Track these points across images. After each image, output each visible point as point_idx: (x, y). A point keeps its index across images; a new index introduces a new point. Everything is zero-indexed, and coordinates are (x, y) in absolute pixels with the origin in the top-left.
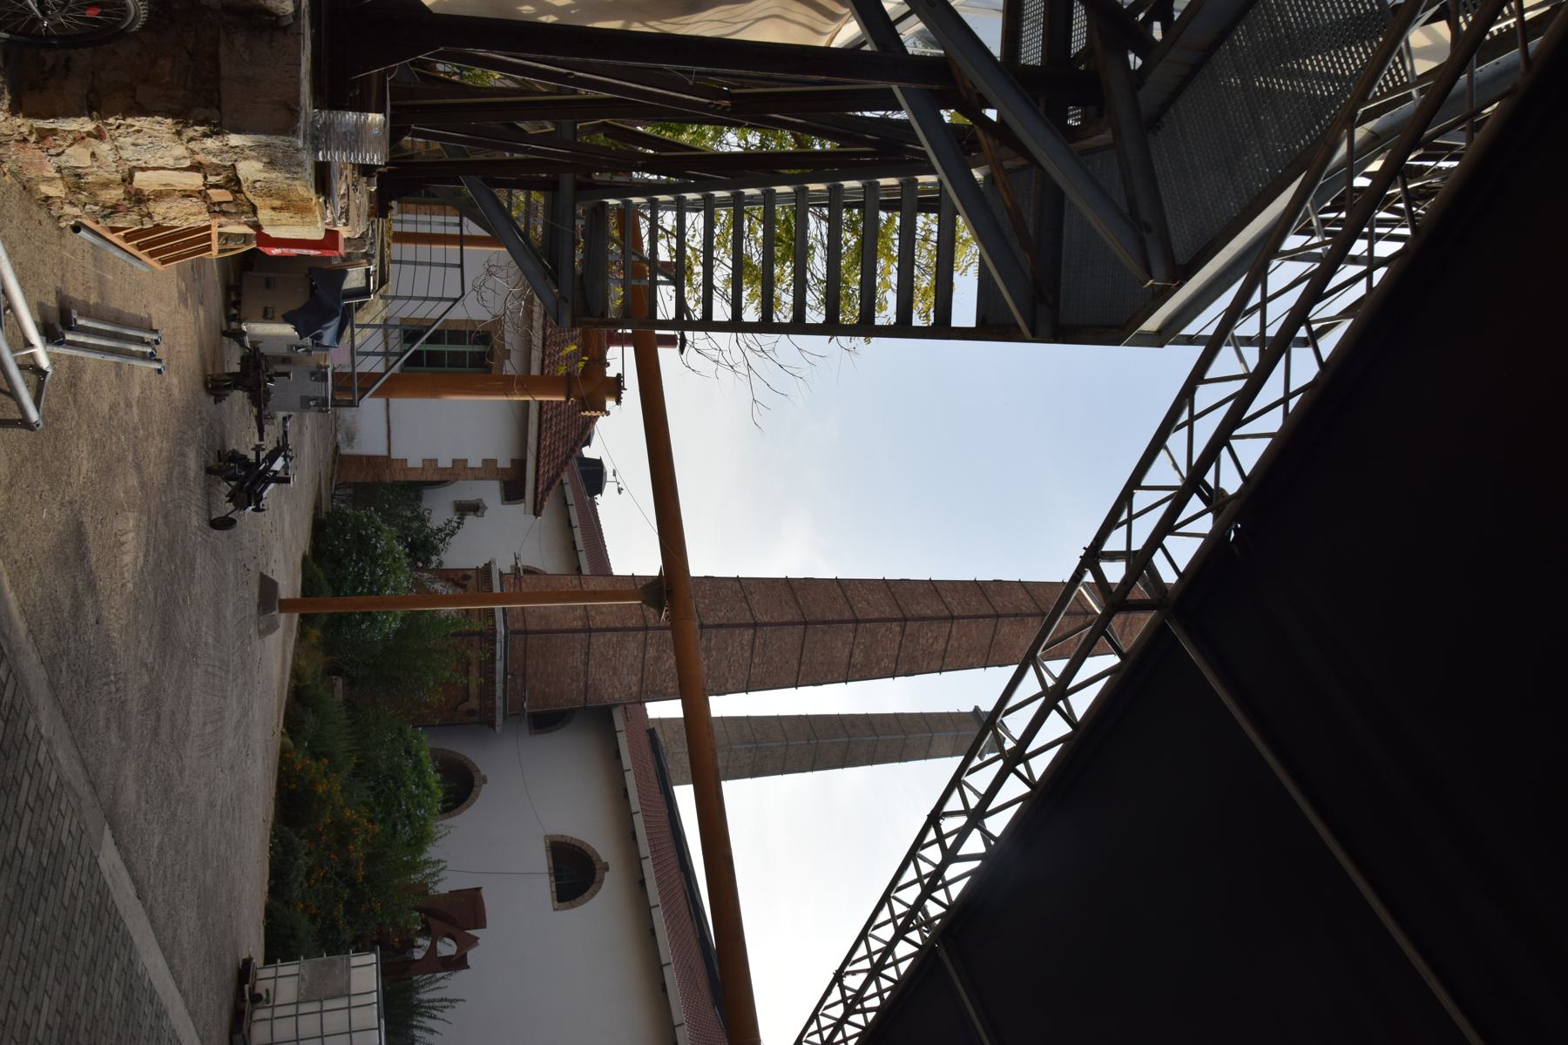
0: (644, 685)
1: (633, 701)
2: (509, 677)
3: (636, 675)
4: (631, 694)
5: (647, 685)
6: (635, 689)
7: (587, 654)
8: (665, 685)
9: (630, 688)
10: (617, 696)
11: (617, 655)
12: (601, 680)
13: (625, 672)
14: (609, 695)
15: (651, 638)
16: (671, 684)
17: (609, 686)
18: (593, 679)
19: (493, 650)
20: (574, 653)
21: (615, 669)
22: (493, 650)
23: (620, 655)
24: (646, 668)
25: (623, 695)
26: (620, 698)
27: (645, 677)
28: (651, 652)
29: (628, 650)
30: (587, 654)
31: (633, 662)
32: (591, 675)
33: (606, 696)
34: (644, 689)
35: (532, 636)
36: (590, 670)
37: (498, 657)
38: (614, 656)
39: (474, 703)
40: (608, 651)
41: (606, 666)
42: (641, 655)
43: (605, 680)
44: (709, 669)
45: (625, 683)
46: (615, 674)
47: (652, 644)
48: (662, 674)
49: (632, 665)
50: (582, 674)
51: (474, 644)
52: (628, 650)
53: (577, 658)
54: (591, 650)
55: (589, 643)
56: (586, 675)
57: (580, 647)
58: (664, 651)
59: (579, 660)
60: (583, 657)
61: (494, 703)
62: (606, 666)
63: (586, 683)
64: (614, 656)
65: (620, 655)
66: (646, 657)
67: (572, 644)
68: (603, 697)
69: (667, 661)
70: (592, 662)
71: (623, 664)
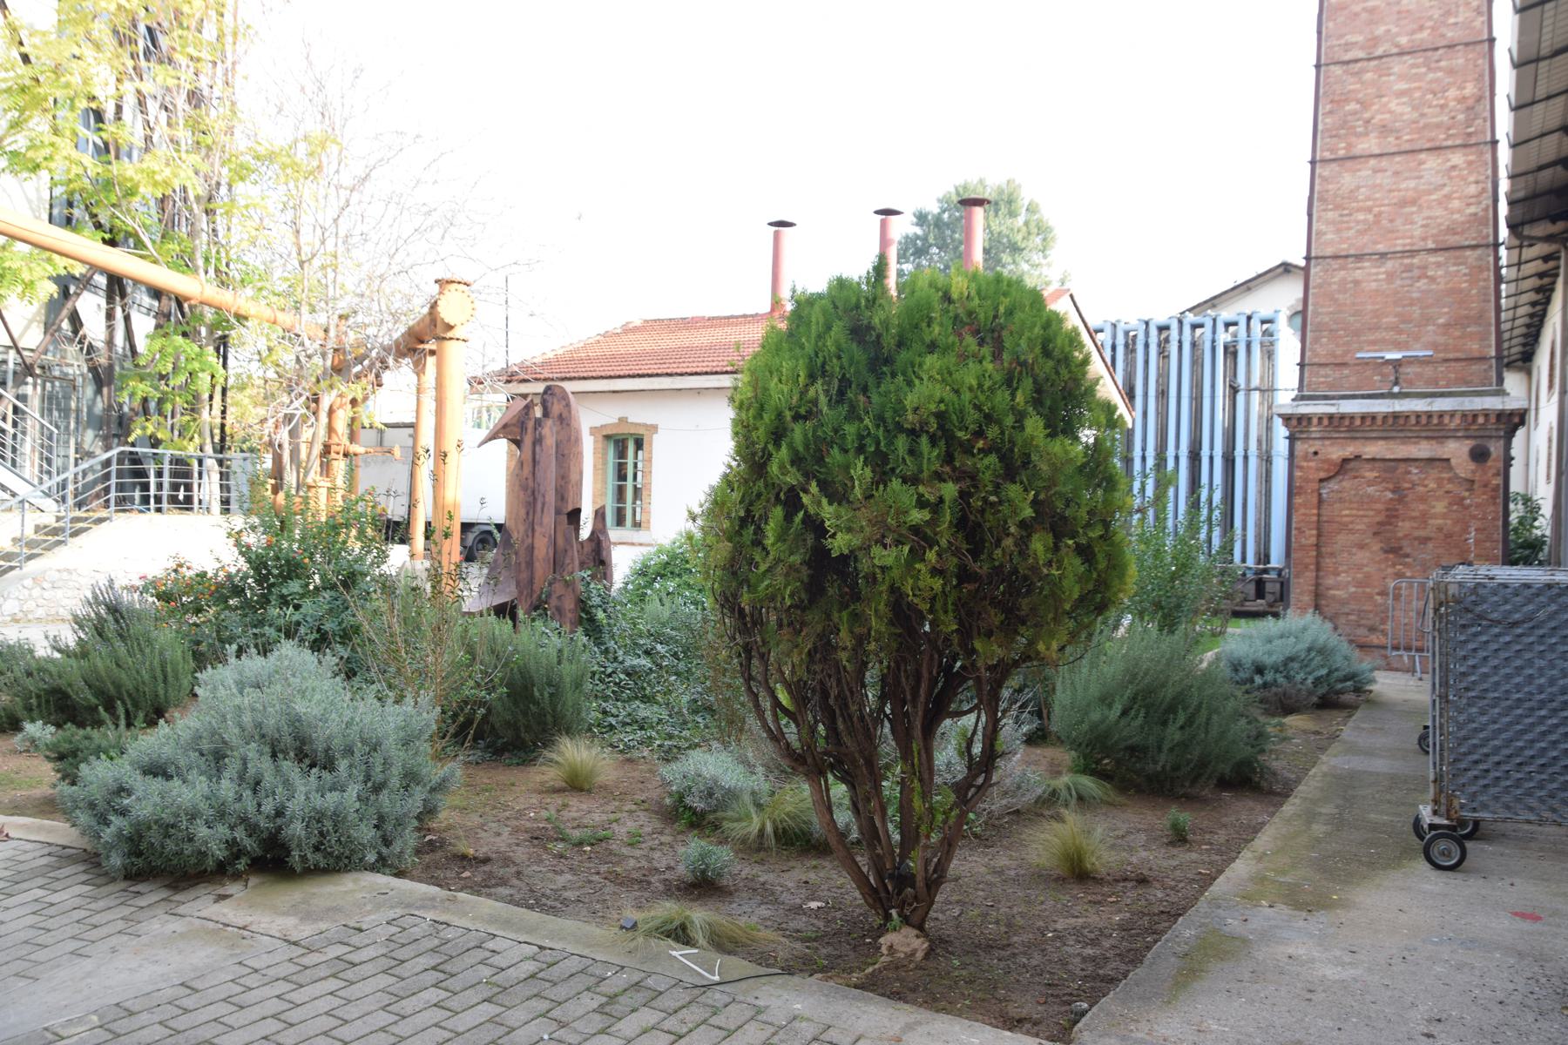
0: (1449, 143)
1: (1488, 157)
2: (1396, 389)
3: (1421, 163)
4: (1470, 163)
5: (1449, 137)
6: (1457, 158)
7: (1359, 257)
8: (1452, 104)
9: (1454, 167)
10: (1473, 189)
11: (1370, 203)
12: (1423, 226)
13: (1412, 184)
14: (1469, 205)
15: (1332, 151)
16: (1452, 93)
17: (1446, 209)
18: (1424, 239)
19: (1320, 419)
20: (1357, 282)
21: (1403, 203)
22: (1320, 419)
23: (1368, 199)
24: (1407, 147)
25: (1472, 179)
26: (1477, 182)
27: (1428, 145)
28: (1370, 144)
29: (1358, 188)
30: (1359, 257)
31: (1389, 173)
32: (1412, 245)
33: (1472, 209)
34: (1458, 142)
35: (1308, 354)
36: (1399, 249)
37: (1332, 410)
38: (1369, 210)
39: (1457, 451)
40: (1358, 222)
41: (1391, 221)
42: (1372, 162)
43: (1428, 218)
44: (1421, 28)
45: (1439, 180)
46: (1413, 202)
47: (1349, 146)
48: (1423, 115)
49: (1396, 173)
50: (1407, 261)
51: (1312, 450)
52: (1358, 188)
53: (1369, 274)
54: (1352, 252)
55: (1336, 257)
56: (1413, 253)
57: (1342, 273)
58: (1368, 122)
59: (1374, 271)
60: (1367, 264)
61: (1452, 414)
62: (1391, 221)
63: (1435, 250)
64: (1369, 210)
65: (1368, 199)
66: (1377, 151)
67: (1335, 287)
68: (1475, 214)
69: (1390, 112)
70: (1381, 248)
71: (1390, 191)
